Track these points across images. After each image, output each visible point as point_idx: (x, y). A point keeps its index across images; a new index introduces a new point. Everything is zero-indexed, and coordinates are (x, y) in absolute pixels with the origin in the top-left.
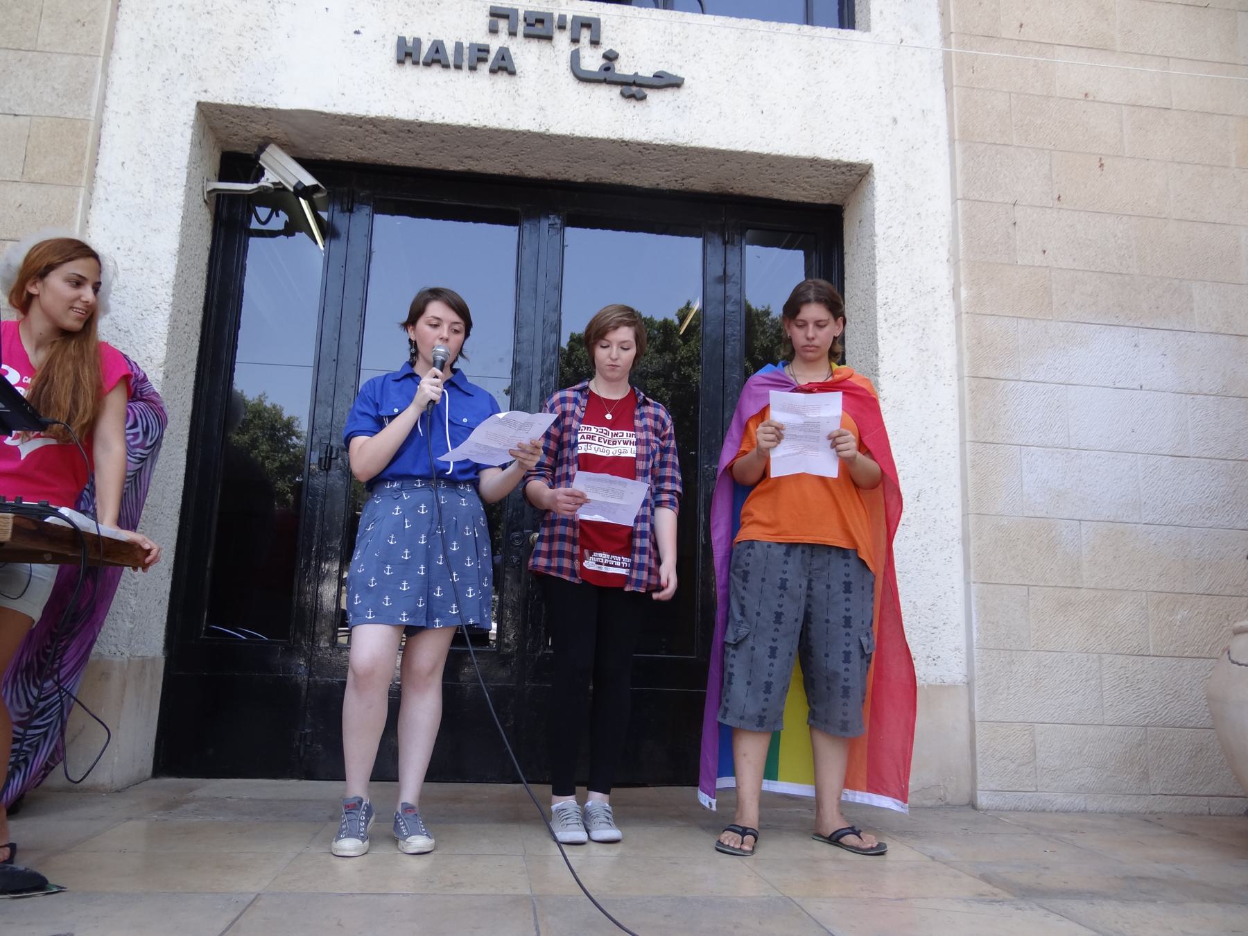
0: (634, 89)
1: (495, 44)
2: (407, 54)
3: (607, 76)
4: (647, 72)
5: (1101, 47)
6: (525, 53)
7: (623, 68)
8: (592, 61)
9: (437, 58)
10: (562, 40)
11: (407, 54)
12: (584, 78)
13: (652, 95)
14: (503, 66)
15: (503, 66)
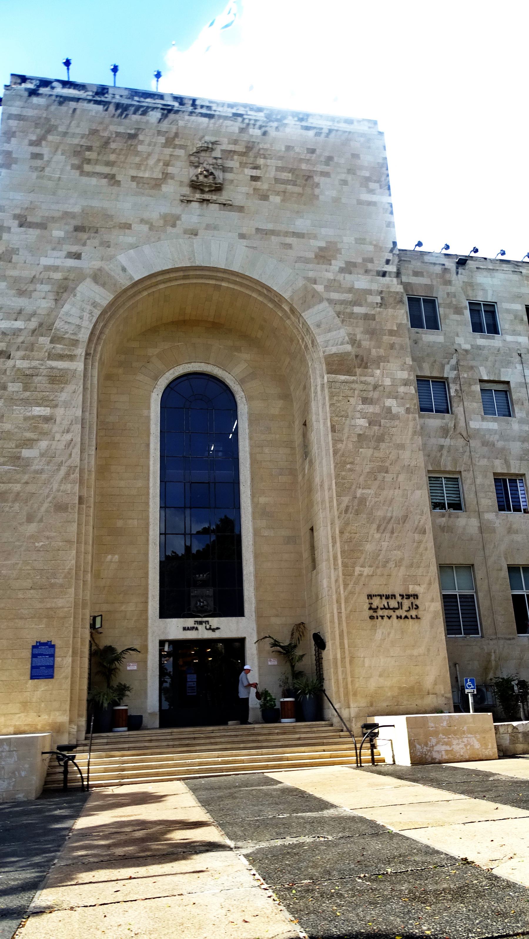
0: (214, 630)
1: (196, 626)
2: (184, 629)
3: (210, 629)
4: (215, 627)
5: (277, 616)
6: (200, 627)
7: (212, 627)
8: (208, 627)
9: (188, 629)
10: (204, 624)
11: (184, 629)
12: (207, 629)
13: (217, 631)
14: (197, 629)
15: (197, 629)
